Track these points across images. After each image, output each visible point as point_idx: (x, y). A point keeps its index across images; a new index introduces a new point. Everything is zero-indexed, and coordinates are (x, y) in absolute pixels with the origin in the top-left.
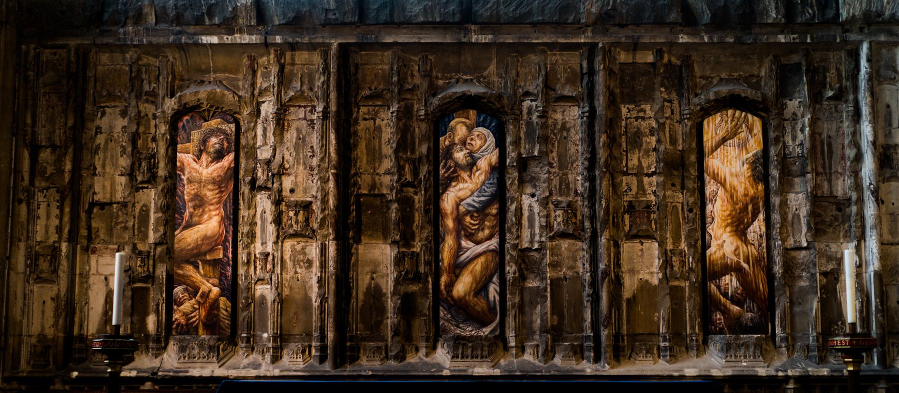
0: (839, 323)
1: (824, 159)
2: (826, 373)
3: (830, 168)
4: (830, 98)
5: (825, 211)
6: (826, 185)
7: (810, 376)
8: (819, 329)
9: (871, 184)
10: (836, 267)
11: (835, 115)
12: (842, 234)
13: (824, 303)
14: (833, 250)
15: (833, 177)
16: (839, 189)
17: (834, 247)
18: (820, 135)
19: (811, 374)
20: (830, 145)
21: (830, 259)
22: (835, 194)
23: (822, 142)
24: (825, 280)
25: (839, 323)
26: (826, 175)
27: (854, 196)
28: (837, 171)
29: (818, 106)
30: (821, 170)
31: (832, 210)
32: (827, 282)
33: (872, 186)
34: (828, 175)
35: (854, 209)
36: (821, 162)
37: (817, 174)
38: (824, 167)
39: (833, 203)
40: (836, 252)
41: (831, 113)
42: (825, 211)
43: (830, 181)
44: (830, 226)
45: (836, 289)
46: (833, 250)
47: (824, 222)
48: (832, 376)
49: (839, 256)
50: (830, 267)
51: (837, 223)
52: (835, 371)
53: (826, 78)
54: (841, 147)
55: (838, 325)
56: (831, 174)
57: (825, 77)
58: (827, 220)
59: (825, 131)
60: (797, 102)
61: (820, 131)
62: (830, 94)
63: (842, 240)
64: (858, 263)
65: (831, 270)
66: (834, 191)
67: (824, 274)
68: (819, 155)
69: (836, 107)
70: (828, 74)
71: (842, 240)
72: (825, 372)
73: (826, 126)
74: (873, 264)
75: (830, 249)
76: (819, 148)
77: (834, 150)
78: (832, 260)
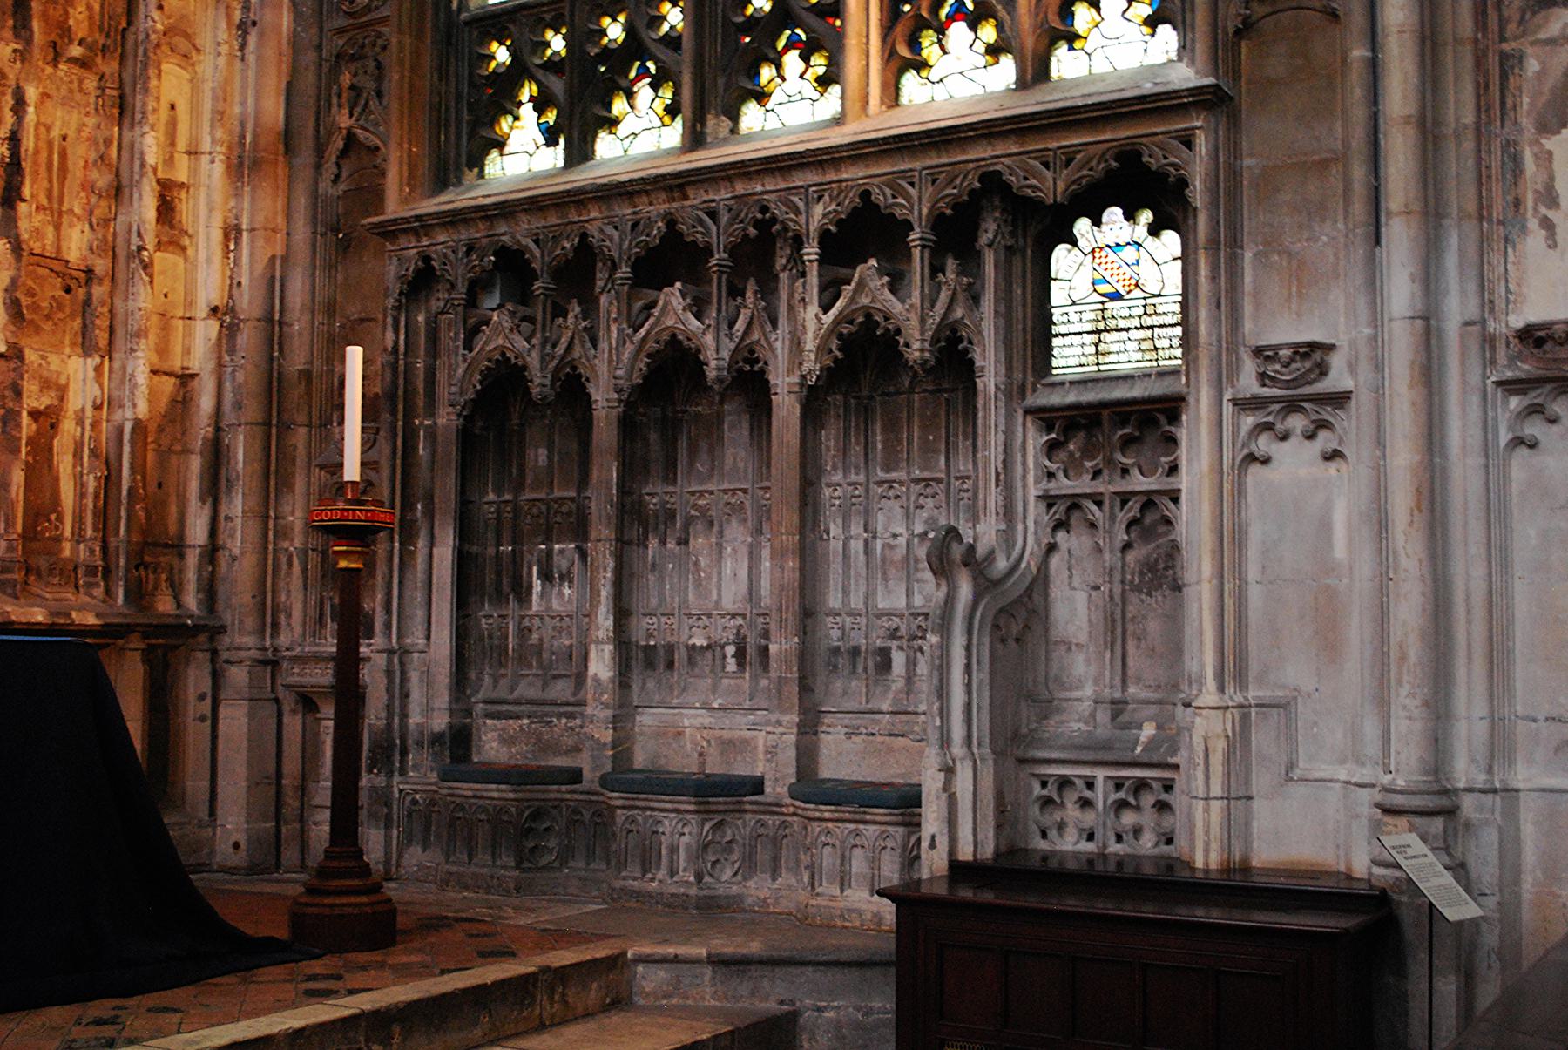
0: (53, 517)
1: (50, 181)
2: (40, 618)
3: (61, 202)
4: (73, 61)
5: (41, 286)
6: (50, 232)
7: (13, 623)
8: (19, 528)
9: (141, 249)
10: (56, 402)
11: (78, 96)
12: (67, 342)
13: (29, 469)
14: (53, 367)
15: (65, 220)
16: (74, 246)
17: (54, 362)
18: (48, 129)
19: (13, 618)
20: (63, 155)
21: (46, 384)
22: (67, 258)
23: (50, 144)
24: (34, 427)
25: (53, 517)
26: (52, 212)
27: (101, 266)
28: (71, 211)
29: (49, 70)
30: (45, 202)
31: (54, 286)
32: (38, 430)
33: (145, 253)
34: (56, 215)
35: (99, 291)
36: (45, 184)
37: (37, 208)
38: (49, 197)
39: (57, 273)
40: (59, 374)
41: (71, 91)
42: (41, 286)
43: (58, 227)
44: (48, 317)
45: (51, 449)
46: (53, 367)
47: (39, 307)
48: (54, 624)
49: (63, 381)
50: (43, 402)
51: (61, 315)
52: (58, 614)
53: (67, 18)
54: (82, 163)
55: (49, 521)
56: (60, 213)
57: (67, 13)
58: (45, 304)
59: (58, 123)
60: (9, 49)
61: (49, 122)
62: (76, 51)
63: (68, 350)
64: (98, 403)
65: (48, 407)
66: (64, 248)
67: (35, 415)
68: (43, 170)
69: (81, 81)
70: (71, 11)
71: (68, 350)
72: (39, 616)
73: (59, 114)
74: (134, 406)
75: (48, 363)
76: (44, 156)
77: (70, 165)
78: (49, 387)
